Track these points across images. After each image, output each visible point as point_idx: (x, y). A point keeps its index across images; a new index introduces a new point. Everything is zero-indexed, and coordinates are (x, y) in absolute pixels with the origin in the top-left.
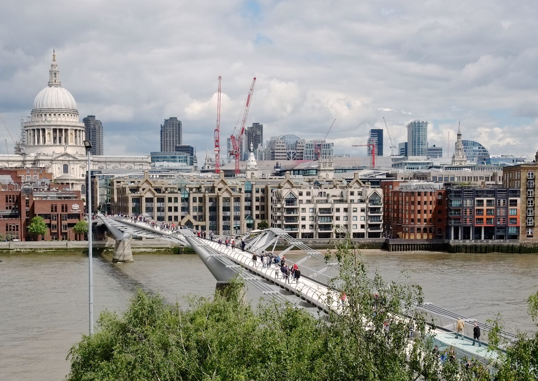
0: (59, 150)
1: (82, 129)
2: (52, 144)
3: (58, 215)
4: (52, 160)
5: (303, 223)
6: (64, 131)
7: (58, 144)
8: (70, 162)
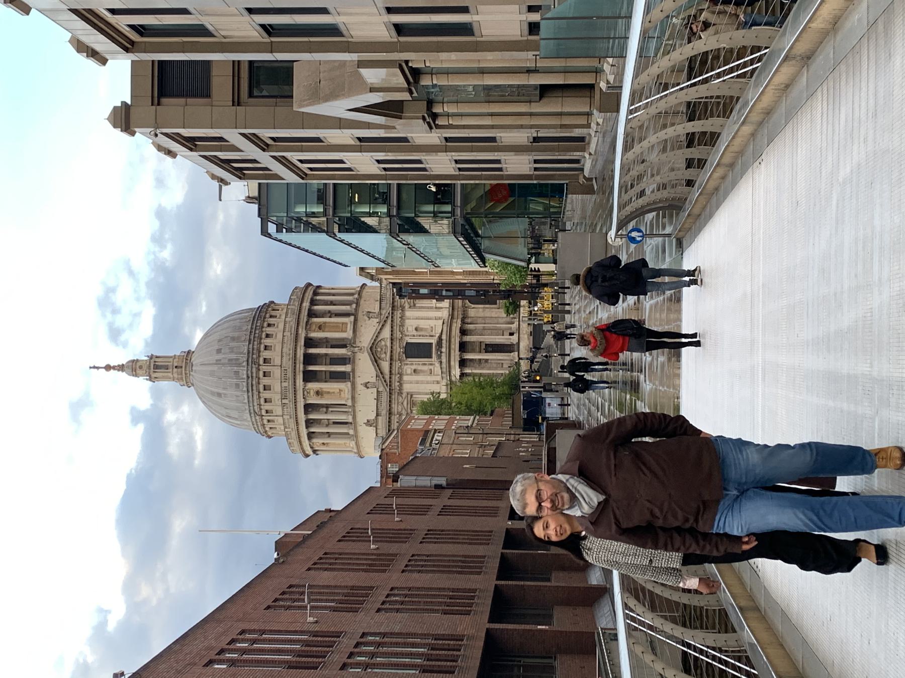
2: (349, 384)
6: (312, 351)
7: (347, 368)
8: (399, 335)
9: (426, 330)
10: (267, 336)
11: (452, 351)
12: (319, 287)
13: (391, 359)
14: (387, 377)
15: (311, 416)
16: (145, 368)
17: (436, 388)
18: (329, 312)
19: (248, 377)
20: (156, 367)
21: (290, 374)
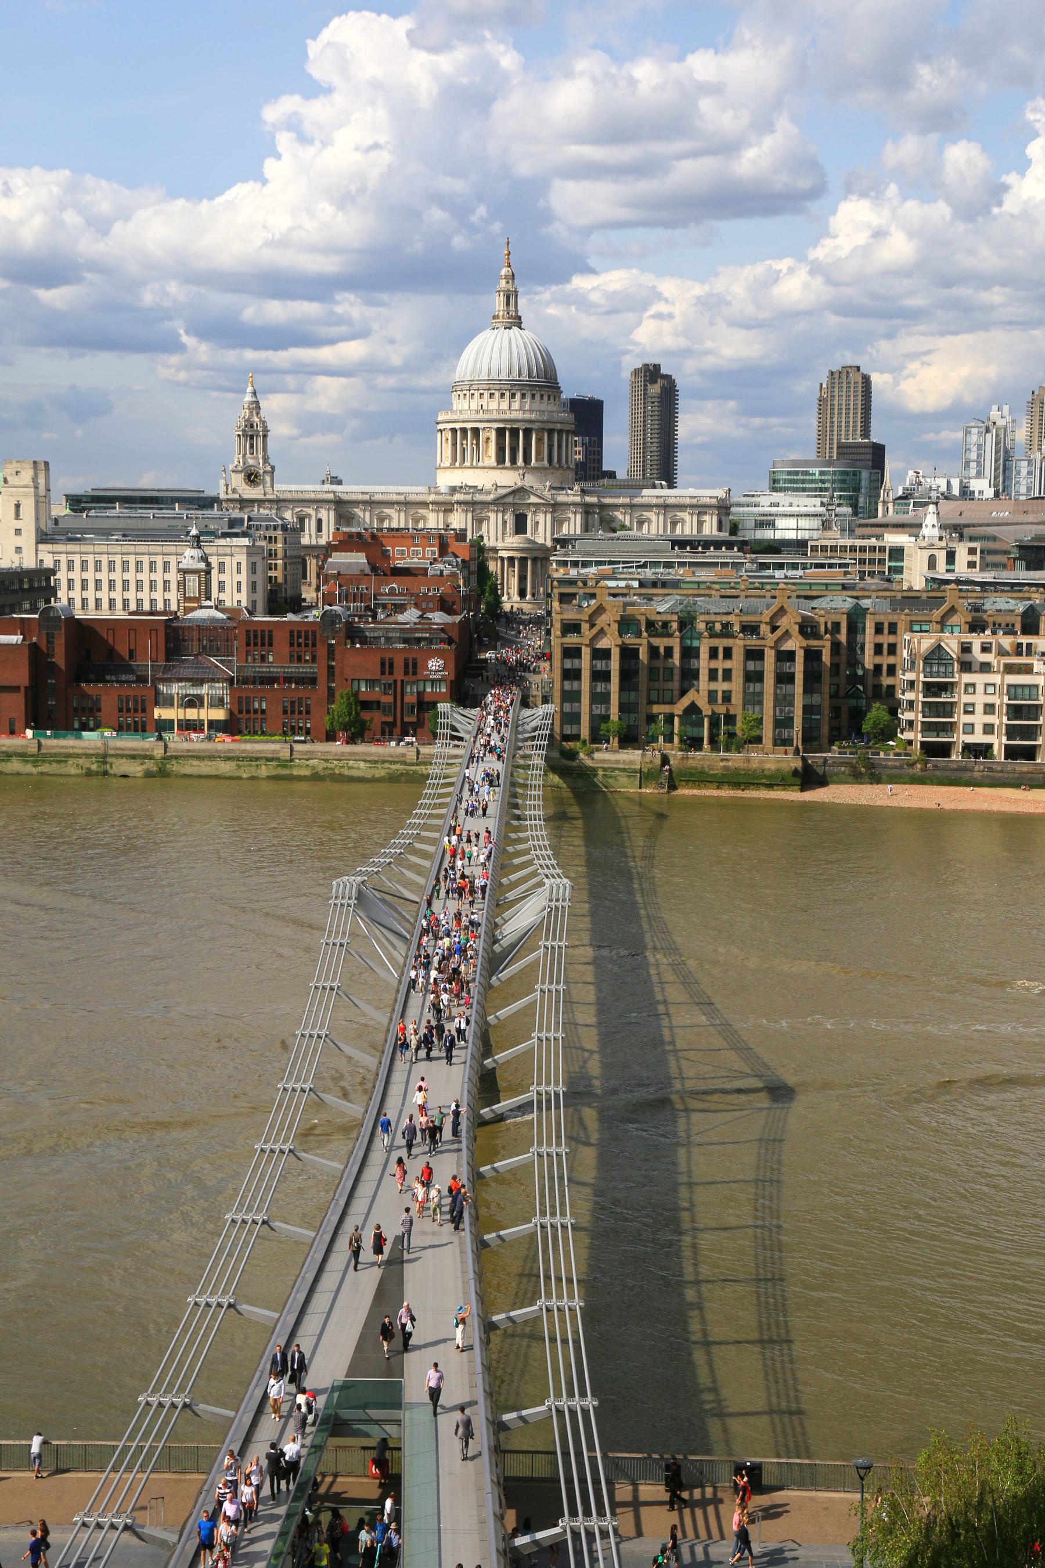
0: (508, 479)
1: (567, 427)
2: (495, 464)
3: (395, 681)
5: (966, 719)
7: (508, 463)
10: (533, 396)
20: (508, 298)
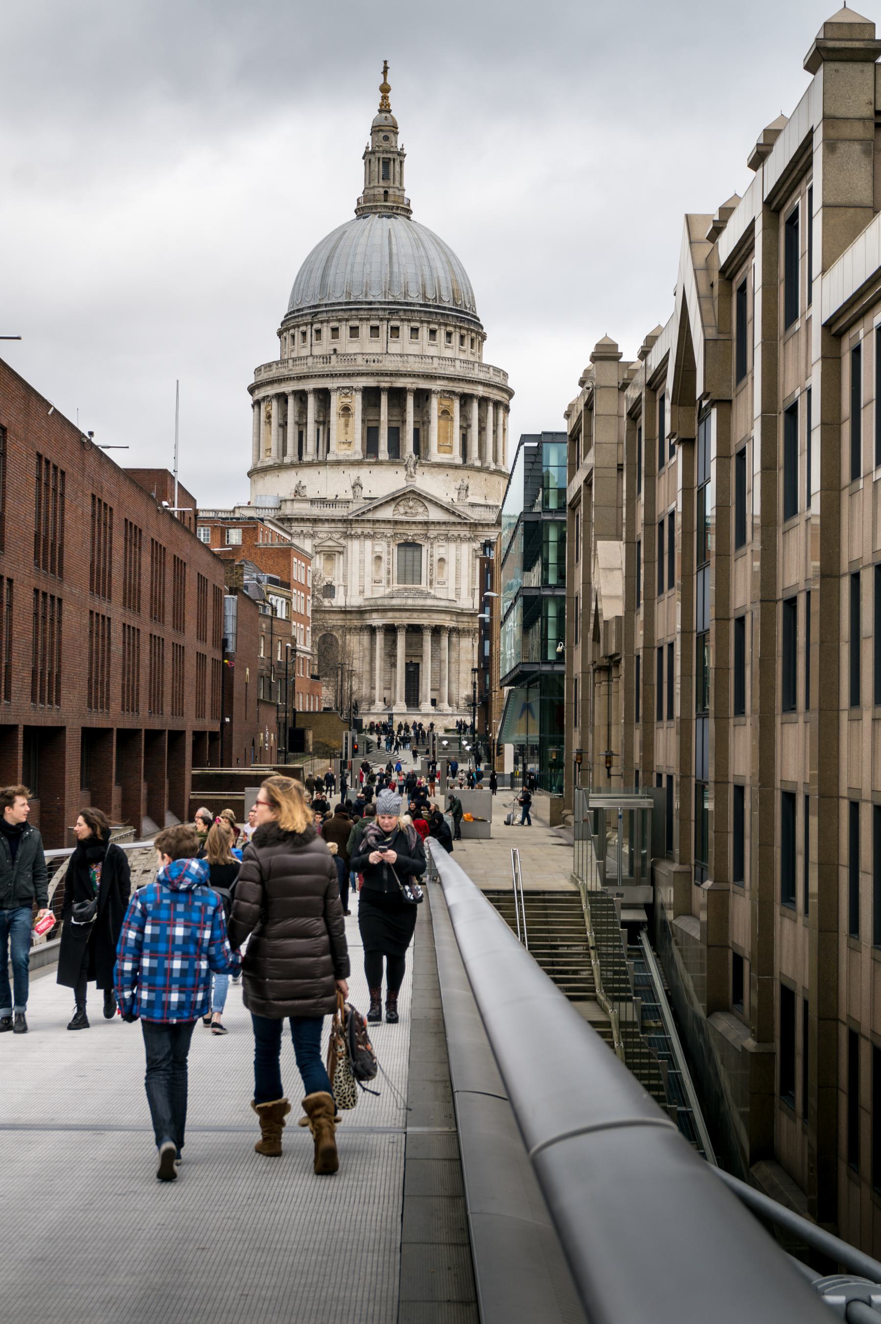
2: (359, 456)
4: (345, 521)
7: (384, 455)
8: (432, 533)
9: (441, 573)
10: (433, 332)
11: (407, 614)
12: (507, 409)
13: (396, 522)
14: (370, 516)
15: (311, 401)
16: (385, 145)
17: (354, 589)
18: (469, 426)
19: (370, 303)
20: (386, 163)
21: (374, 367)
